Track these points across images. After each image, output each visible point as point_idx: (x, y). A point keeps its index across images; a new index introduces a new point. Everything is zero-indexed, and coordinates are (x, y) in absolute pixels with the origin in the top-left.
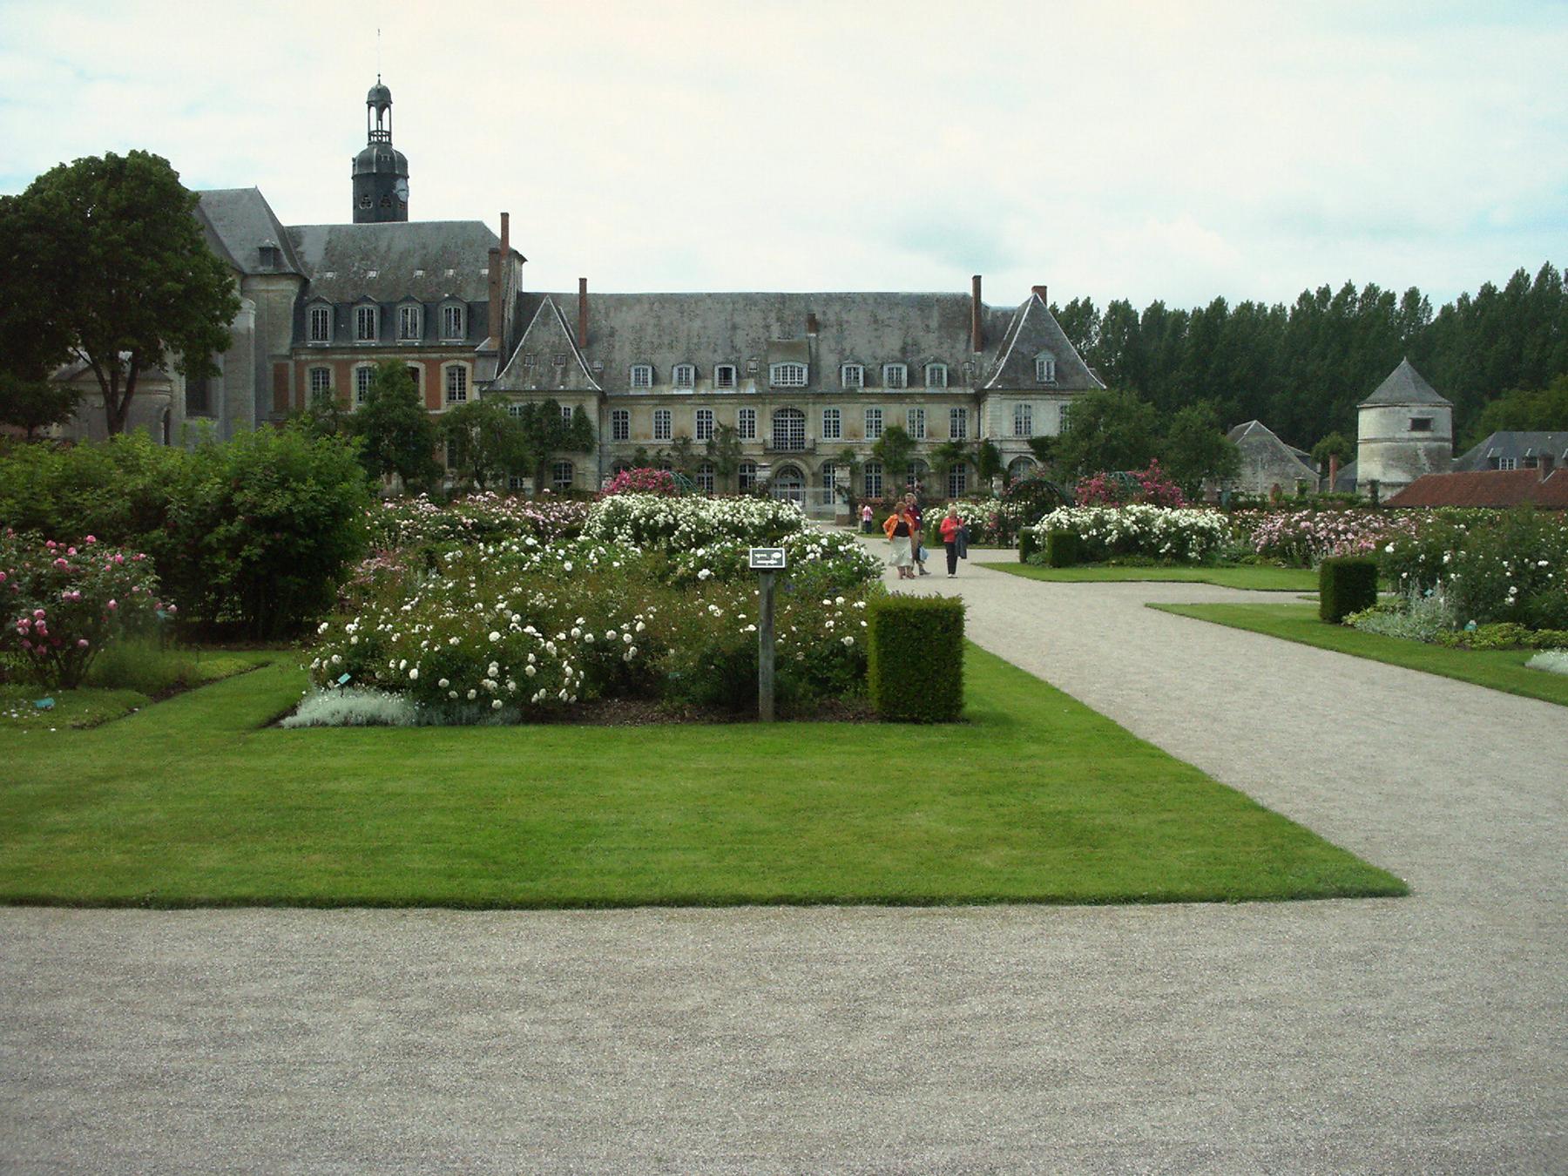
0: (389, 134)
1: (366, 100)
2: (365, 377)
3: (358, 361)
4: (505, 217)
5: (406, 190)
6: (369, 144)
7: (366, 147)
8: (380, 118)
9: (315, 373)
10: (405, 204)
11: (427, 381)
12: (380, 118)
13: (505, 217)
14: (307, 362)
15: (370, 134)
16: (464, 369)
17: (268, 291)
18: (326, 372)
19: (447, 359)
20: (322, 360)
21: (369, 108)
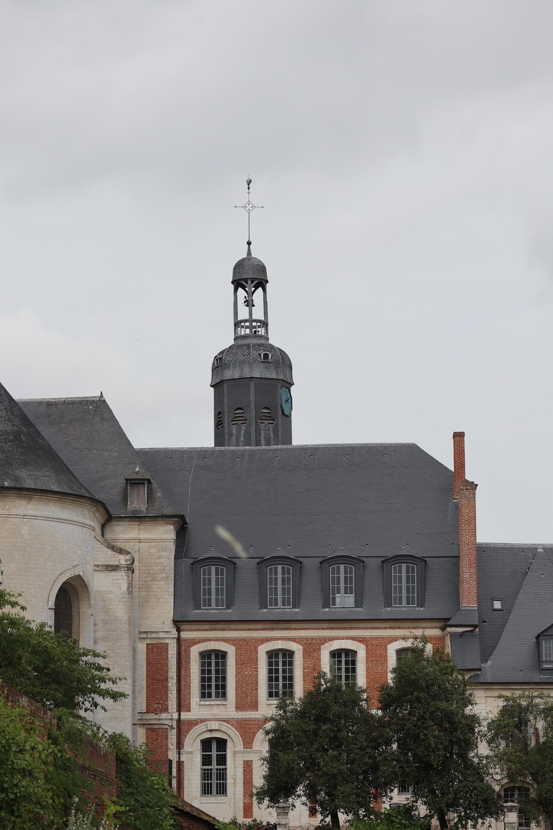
0: (265, 324)
1: (231, 279)
2: (277, 663)
3: (268, 640)
4: (459, 437)
5: (289, 400)
6: (235, 339)
7: (232, 342)
8: (249, 303)
9: (205, 655)
10: (289, 417)
11: (368, 668)
12: (249, 303)
13: (459, 437)
14: (195, 642)
15: (237, 324)
16: (355, 653)
17: (140, 541)
18: (222, 655)
19: (396, 639)
20: (217, 640)
21: (236, 291)
